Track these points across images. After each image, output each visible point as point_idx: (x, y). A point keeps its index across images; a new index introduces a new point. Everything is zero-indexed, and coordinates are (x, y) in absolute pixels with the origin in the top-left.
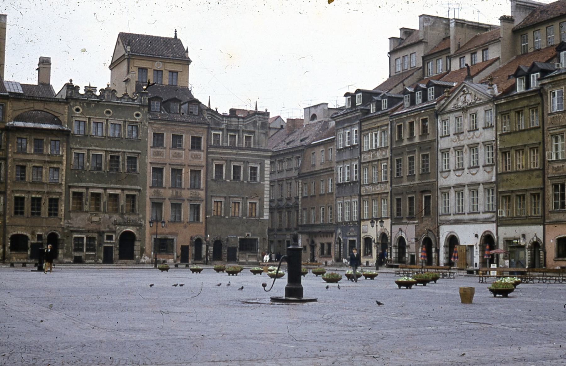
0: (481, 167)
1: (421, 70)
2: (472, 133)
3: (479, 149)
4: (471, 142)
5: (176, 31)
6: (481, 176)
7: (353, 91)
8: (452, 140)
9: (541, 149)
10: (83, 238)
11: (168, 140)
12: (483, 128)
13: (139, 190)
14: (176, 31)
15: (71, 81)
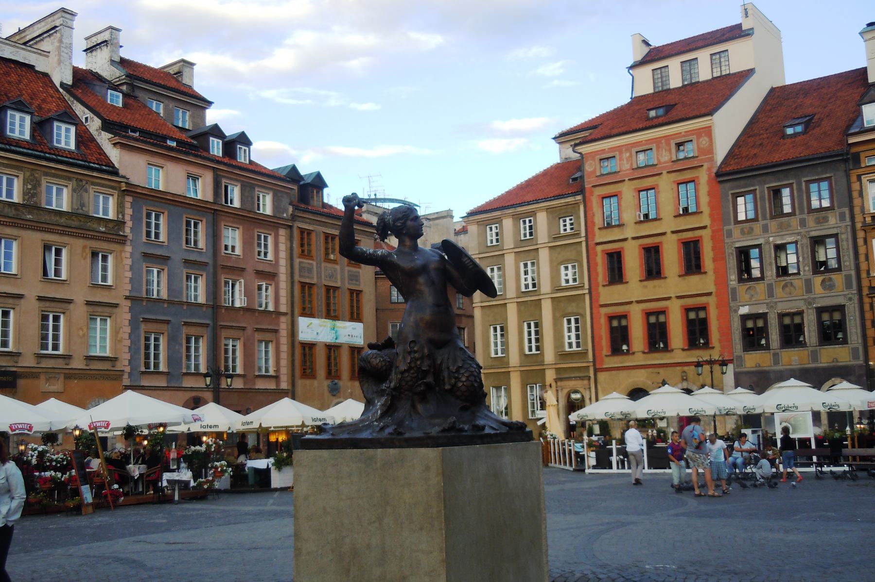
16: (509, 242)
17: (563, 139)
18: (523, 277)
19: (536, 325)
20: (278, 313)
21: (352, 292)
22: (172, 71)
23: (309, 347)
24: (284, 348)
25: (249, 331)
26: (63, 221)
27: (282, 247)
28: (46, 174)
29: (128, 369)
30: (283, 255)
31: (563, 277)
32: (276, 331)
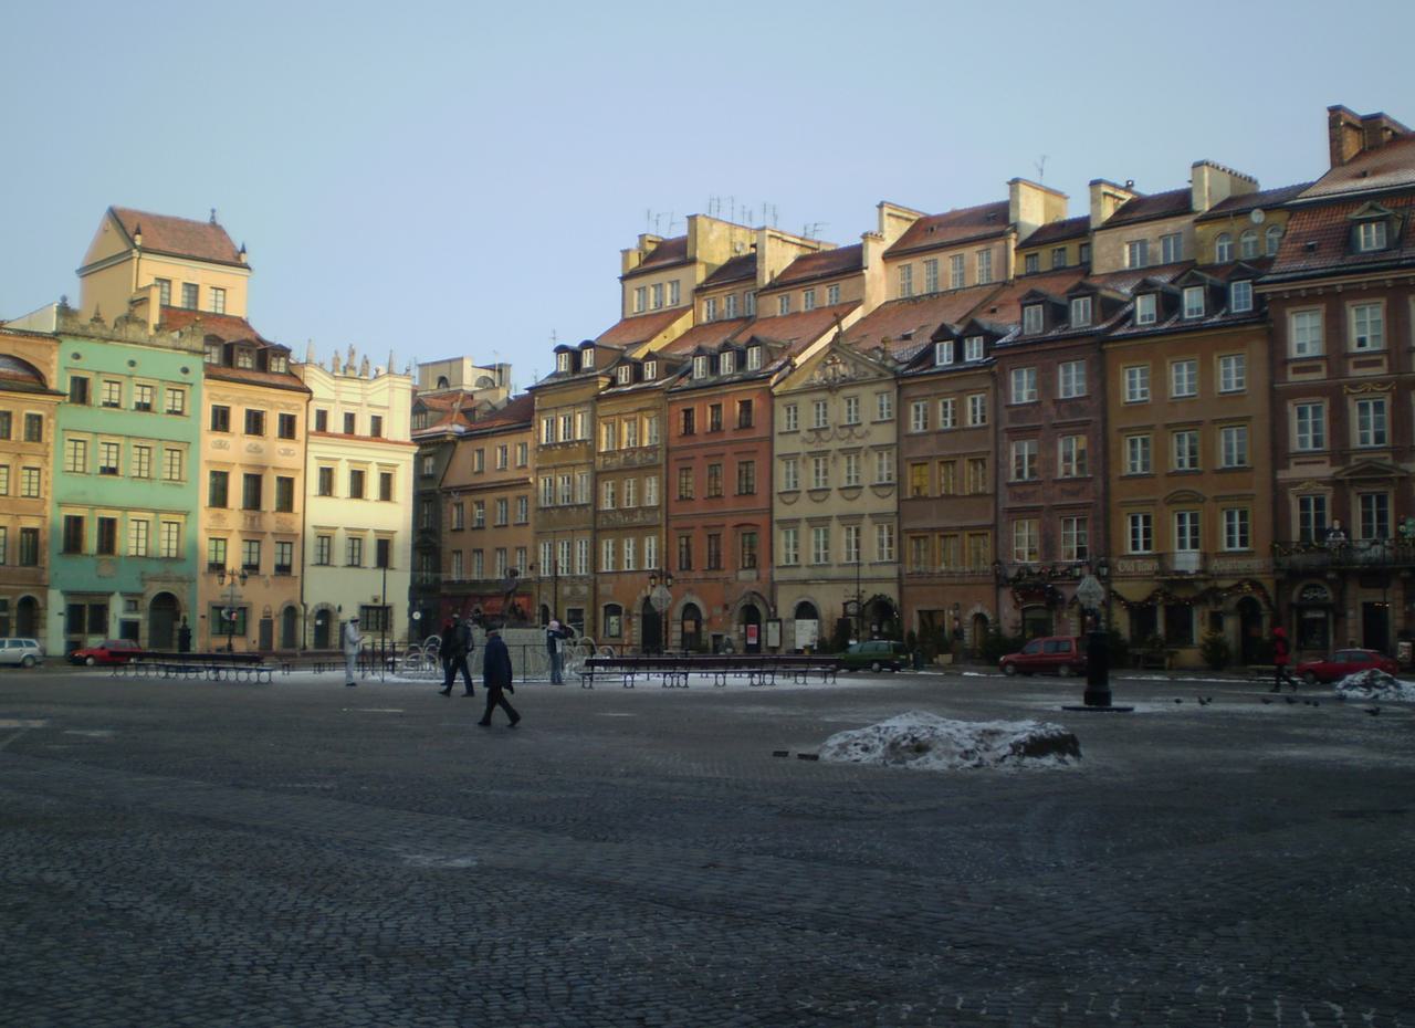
0: (867, 491)
1: (691, 312)
2: (847, 431)
3: (862, 457)
4: (843, 445)
5: (213, 211)
6: (868, 503)
7: (575, 343)
8: (804, 440)
9: (990, 462)
10: (84, 606)
11: (238, 420)
12: (874, 423)
13: (186, 514)
14: (213, 211)
15: (64, 299)
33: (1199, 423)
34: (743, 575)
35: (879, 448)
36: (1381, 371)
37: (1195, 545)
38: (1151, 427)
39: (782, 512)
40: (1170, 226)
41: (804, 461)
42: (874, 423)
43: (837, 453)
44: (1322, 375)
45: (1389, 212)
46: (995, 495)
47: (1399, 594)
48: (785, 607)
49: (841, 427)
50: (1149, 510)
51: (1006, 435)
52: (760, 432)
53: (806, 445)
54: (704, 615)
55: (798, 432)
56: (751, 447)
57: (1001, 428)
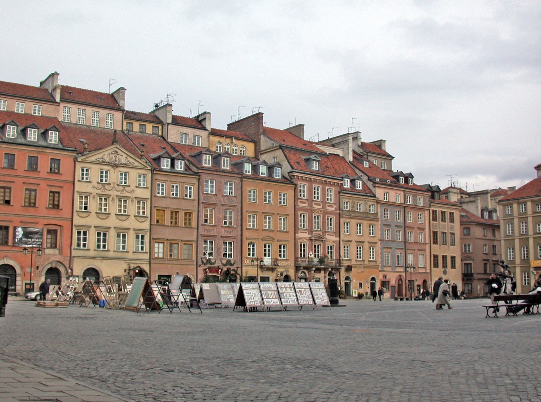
0: (132, 217)
2: (121, 188)
4: (119, 194)
6: (132, 223)
12: (136, 187)
16: (516, 213)
17: (538, 169)
18: (521, 227)
19: (527, 248)
20: (425, 244)
21: (451, 233)
22: (378, 144)
23: (436, 257)
24: (428, 257)
25: (416, 250)
26: (361, 215)
27: (427, 218)
28: (357, 200)
29: (380, 265)
30: (427, 221)
31: (538, 229)
32: (425, 250)
33: (273, 214)
34: (47, 251)
35: (139, 199)
36: (320, 207)
37: (269, 256)
38: (258, 212)
39: (77, 221)
40: (198, 132)
41: (94, 197)
42: (136, 187)
43: (115, 197)
44: (306, 205)
45: (320, 159)
46: (198, 229)
47: (323, 275)
48: (79, 268)
49: (118, 185)
50: (231, 240)
51: (202, 205)
52: (66, 176)
53: (95, 189)
54: (18, 271)
55: (91, 182)
56: (36, 181)
57: (200, 202)
